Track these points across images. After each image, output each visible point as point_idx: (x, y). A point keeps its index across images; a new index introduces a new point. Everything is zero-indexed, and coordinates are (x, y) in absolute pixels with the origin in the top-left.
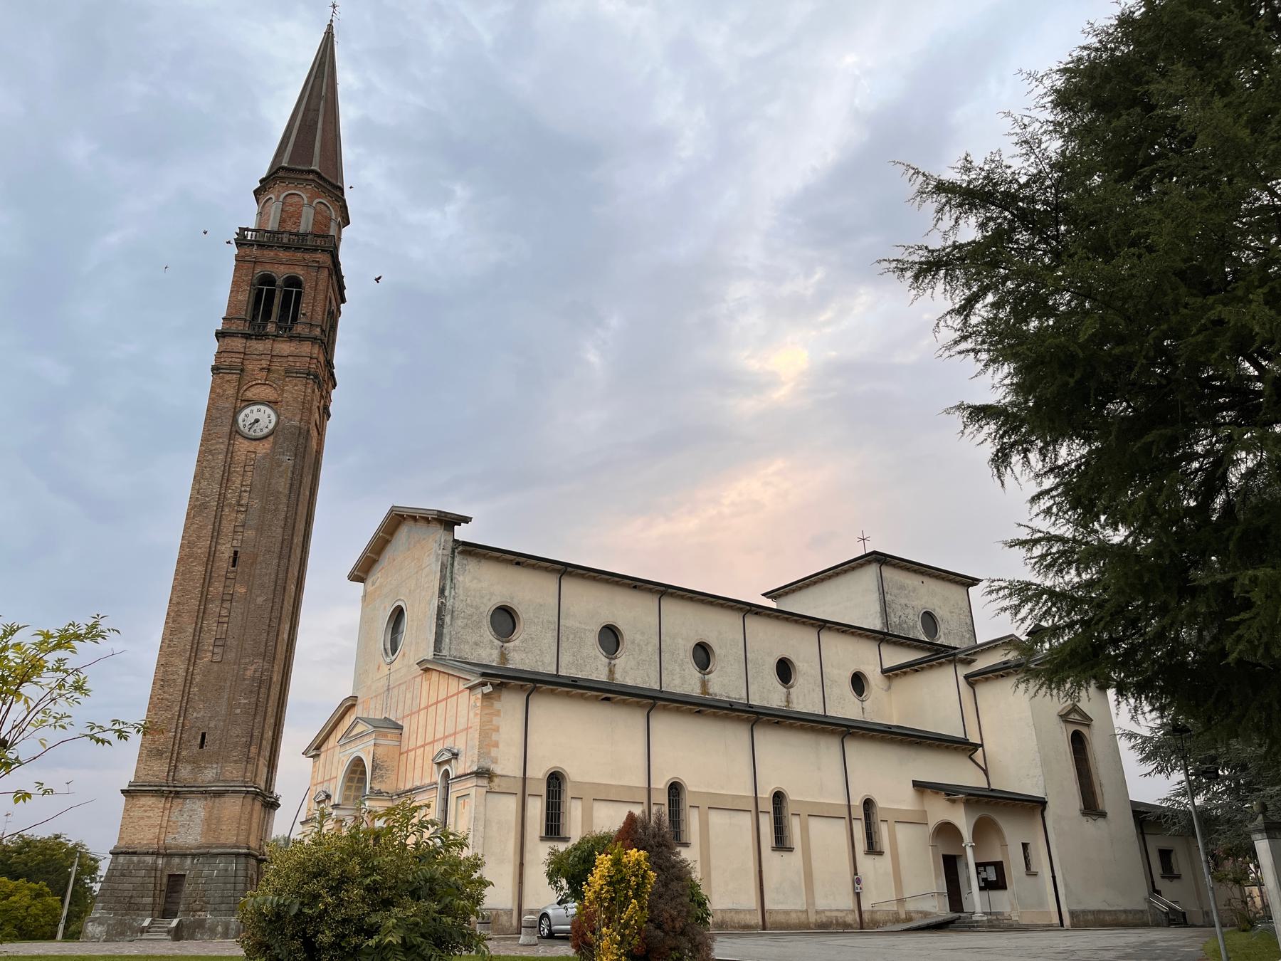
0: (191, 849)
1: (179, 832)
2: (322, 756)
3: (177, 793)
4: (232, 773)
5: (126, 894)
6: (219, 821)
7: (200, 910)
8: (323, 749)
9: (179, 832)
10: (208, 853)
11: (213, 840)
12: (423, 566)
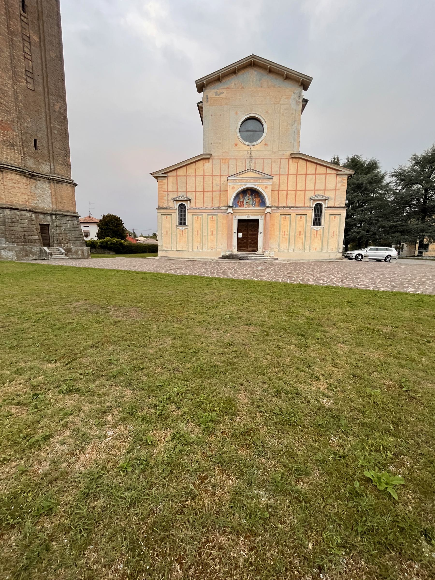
0: (49, 211)
1: (38, 200)
2: (170, 179)
3: (33, 175)
4: (61, 170)
5: (20, 233)
6: (61, 198)
7: (67, 244)
8: (169, 174)
9: (38, 200)
10: (62, 214)
11: (61, 208)
12: (281, 102)
